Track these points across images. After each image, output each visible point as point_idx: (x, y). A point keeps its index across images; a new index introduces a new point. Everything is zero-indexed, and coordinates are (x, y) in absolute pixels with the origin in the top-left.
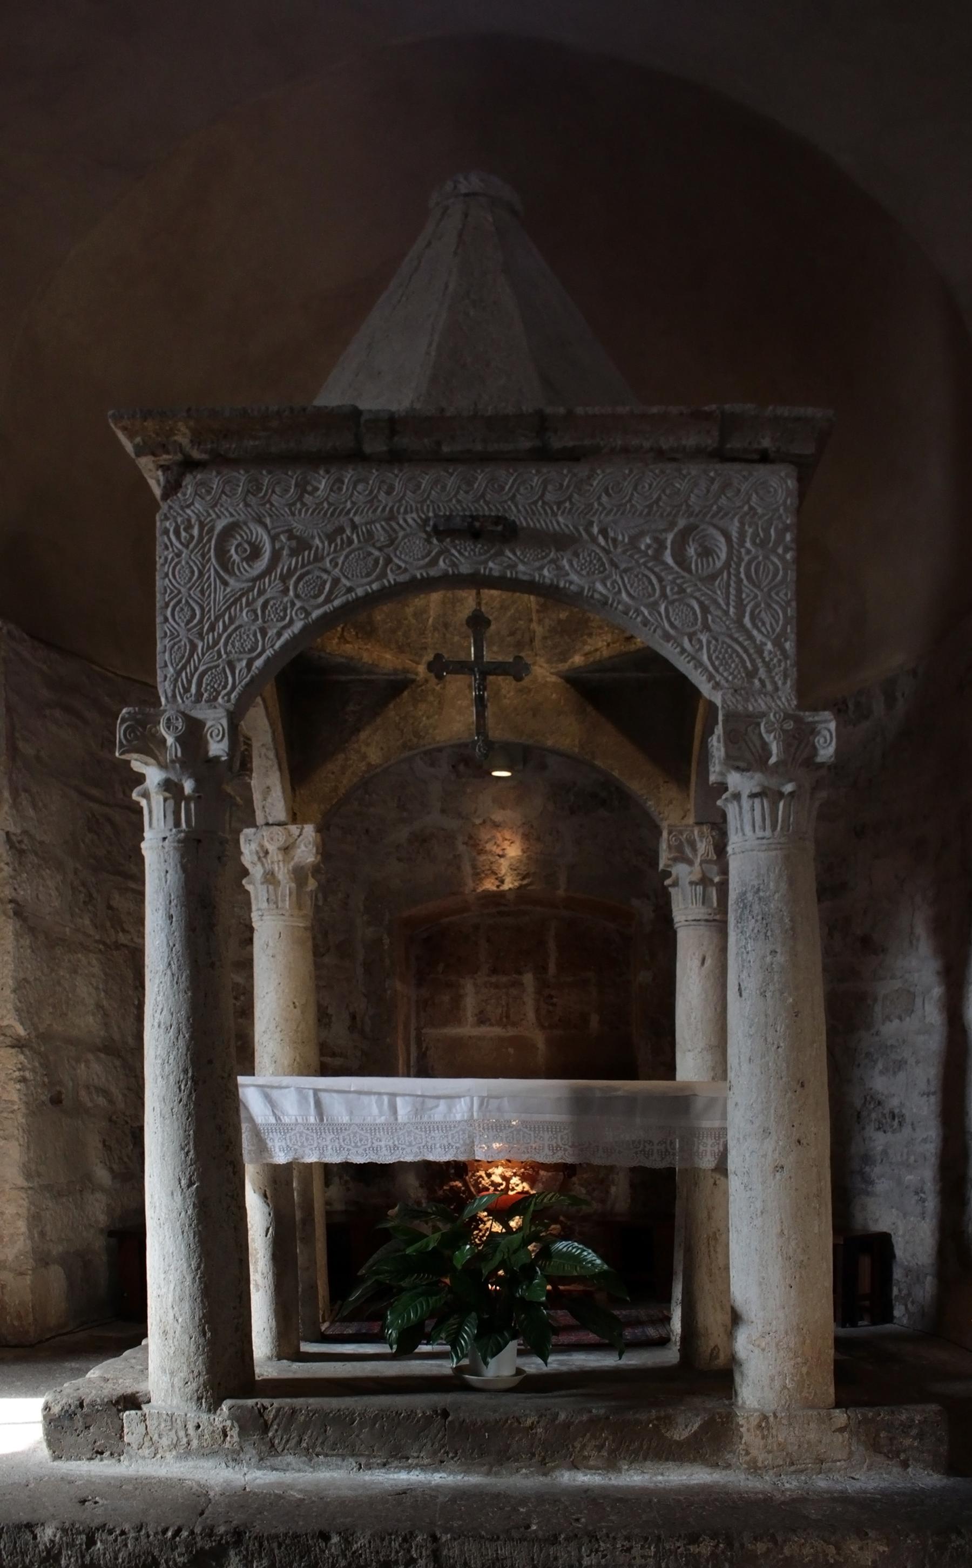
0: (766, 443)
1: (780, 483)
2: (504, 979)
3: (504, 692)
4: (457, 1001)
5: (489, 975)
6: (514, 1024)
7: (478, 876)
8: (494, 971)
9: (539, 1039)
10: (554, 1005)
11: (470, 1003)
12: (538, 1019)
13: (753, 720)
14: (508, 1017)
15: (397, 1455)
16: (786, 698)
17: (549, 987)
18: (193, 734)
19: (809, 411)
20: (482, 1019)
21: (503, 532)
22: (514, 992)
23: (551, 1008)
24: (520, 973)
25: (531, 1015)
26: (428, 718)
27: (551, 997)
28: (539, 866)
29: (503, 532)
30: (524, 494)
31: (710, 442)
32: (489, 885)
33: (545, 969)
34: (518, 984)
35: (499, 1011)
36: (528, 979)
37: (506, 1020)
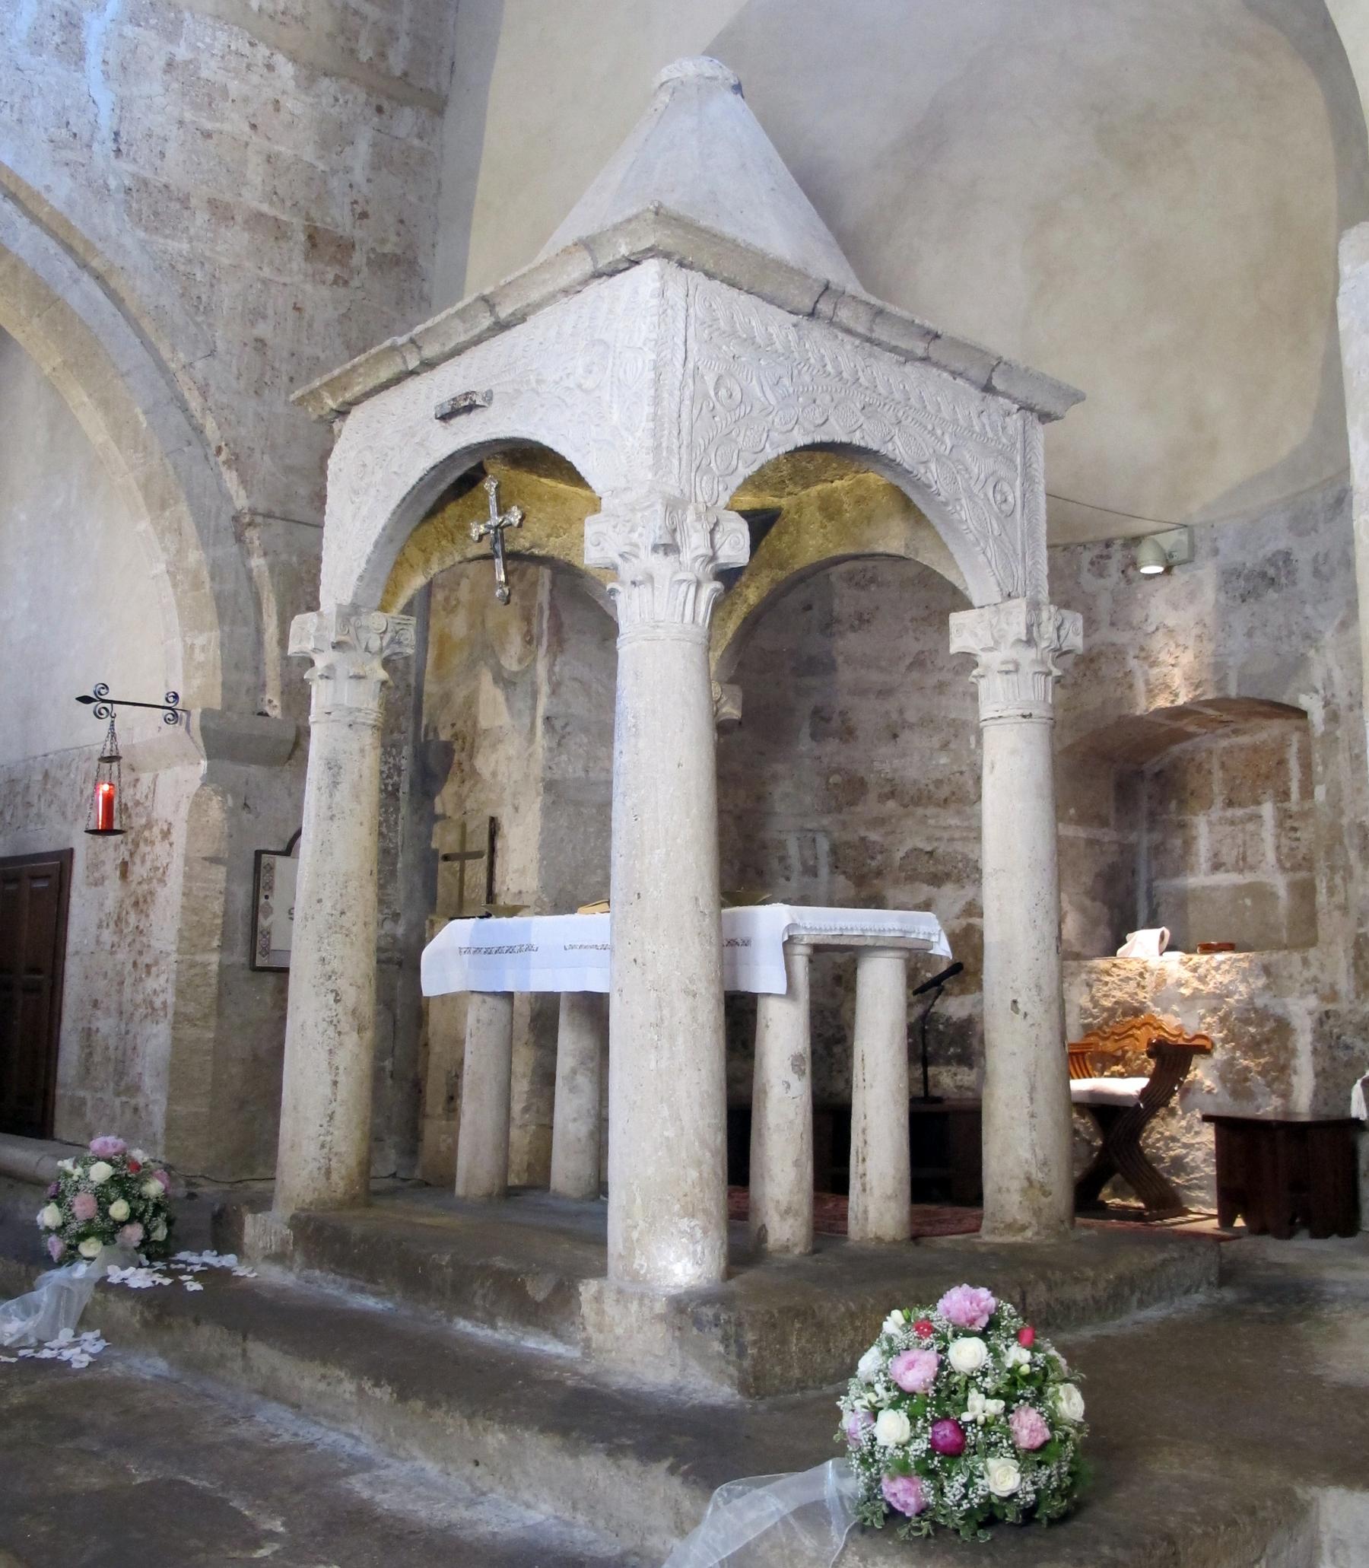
0: (624, 250)
2: (1239, 812)
3: (845, 506)
5: (1223, 809)
6: (1252, 868)
7: (1151, 693)
8: (1230, 803)
10: (1298, 839)
11: (1203, 846)
12: (1279, 861)
14: (1244, 859)
17: (1291, 817)
22: (1251, 827)
23: (1294, 844)
24: (1258, 803)
25: (1271, 856)
27: (1295, 829)
31: (588, 267)
33: (1286, 795)
34: (1257, 818)
35: (1234, 853)
36: (1267, 810)
37: (1243, 863)
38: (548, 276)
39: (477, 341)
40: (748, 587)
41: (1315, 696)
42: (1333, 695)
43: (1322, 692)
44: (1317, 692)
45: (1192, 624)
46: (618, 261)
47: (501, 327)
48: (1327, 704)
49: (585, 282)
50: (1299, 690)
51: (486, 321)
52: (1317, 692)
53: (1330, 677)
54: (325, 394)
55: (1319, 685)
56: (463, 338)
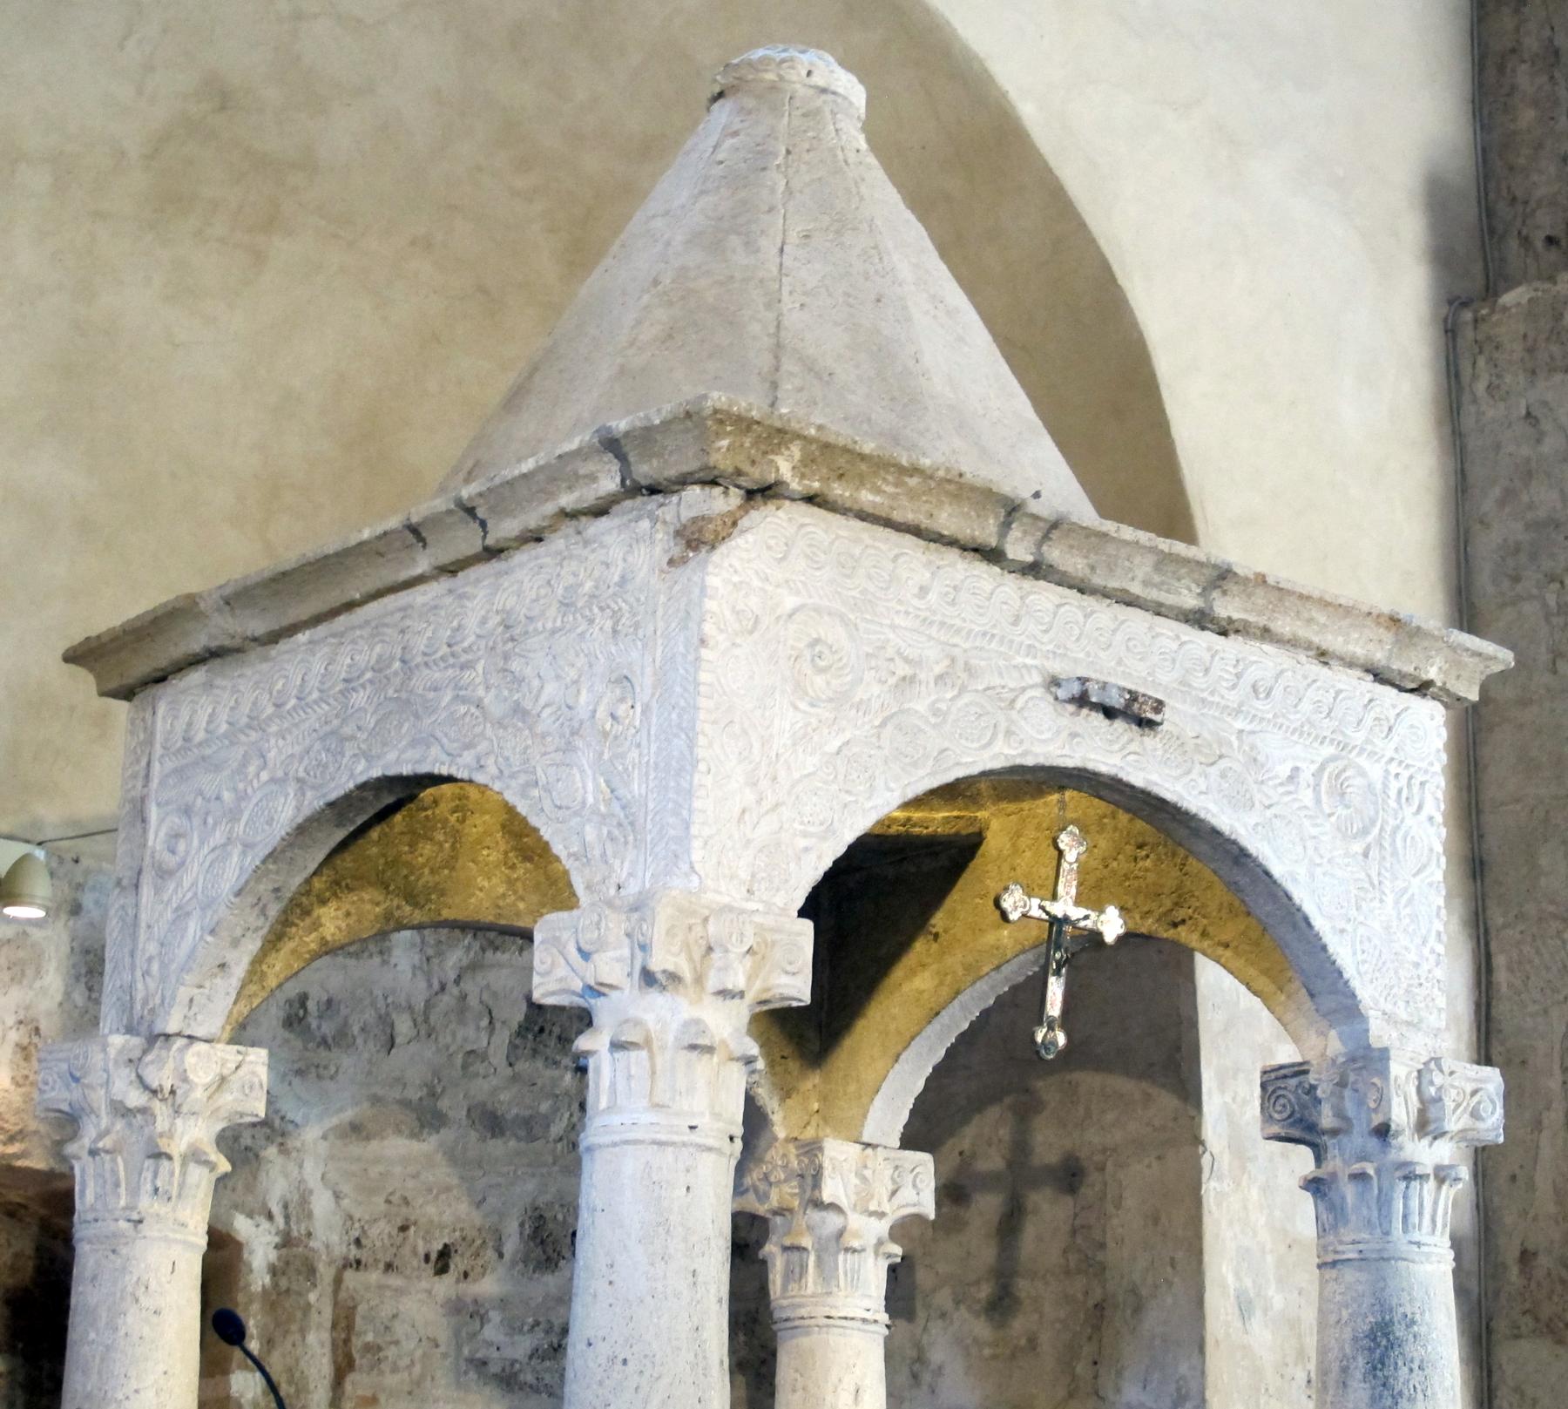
0: (1432, 673)
19: (1488, 647)
26: (432, 872)
31: (1379, 656)
38: (1322, 619)
39: (1159, 610)
40: (323, 902)
41: (265, 1224)
42: (309, 1234)
43: (280, 1220)
44: (270, 1217)
45: (11, 1020)
46: (1413, 678)
47: (1199, 619)
48: (286, 1241)
49: (1351, 664)
50: (236, 1207)
51: (1189, 600)
52: (270, 1217)
53: (304, 1200)
54: (796, 450)
55: (276, 1210)
56: (1136, 589)
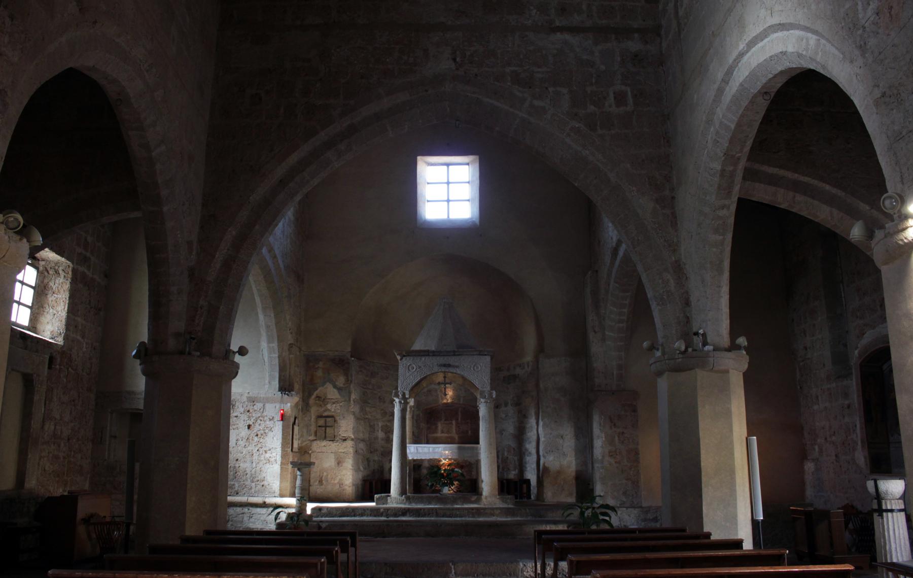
1: (488, 358)
4: (437, 427)
7: (442, 399)
9: (456, 437)
13: (484, 392)
15: (430, 503)
16: (489, 388)
18: (404, 395)
20: (442, 432)
21: (449, 366)
28: (457, 397)
29: (449, 366)
30: (452, 360)
32: (445, 401)
36: (454, 422)
37: (448, 432)
